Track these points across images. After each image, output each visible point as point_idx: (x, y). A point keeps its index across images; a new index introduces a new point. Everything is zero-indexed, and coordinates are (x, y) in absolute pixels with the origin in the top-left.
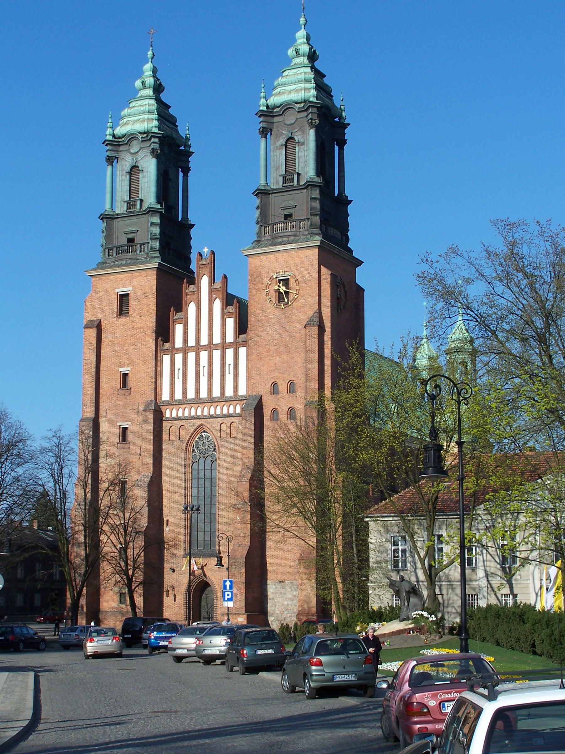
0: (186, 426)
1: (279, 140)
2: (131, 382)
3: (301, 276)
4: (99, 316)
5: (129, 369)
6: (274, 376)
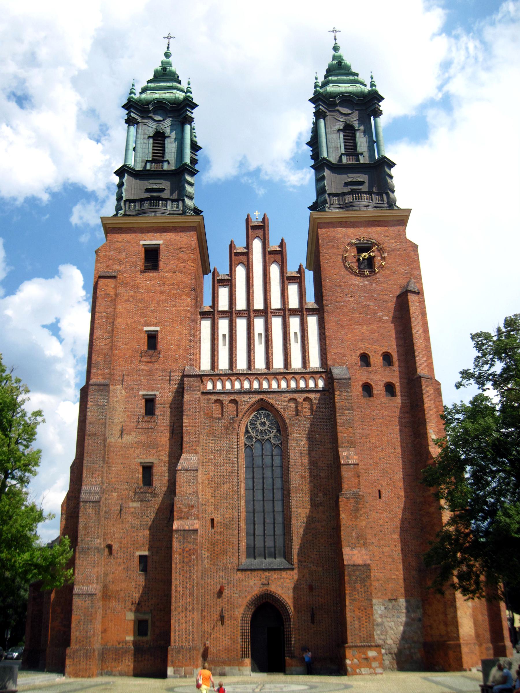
0: (239, 400)
1: (335, 125)
2: (161, 344)
3: (386, 244)
5: (158, 329)
6: (363, 347)
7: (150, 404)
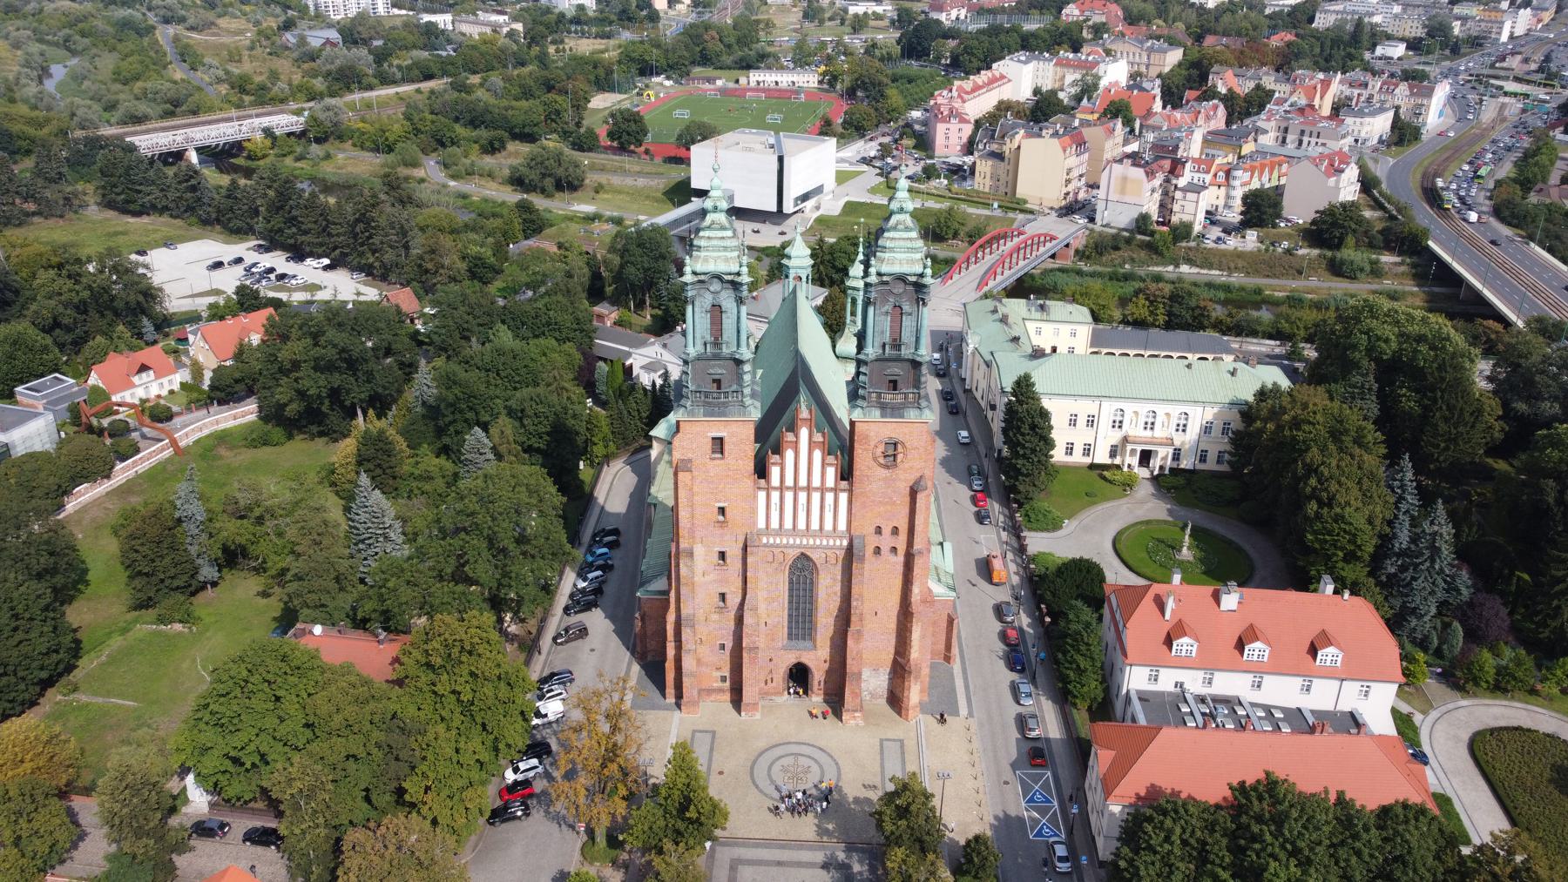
4: (690, 455)
7: (722, 555)
